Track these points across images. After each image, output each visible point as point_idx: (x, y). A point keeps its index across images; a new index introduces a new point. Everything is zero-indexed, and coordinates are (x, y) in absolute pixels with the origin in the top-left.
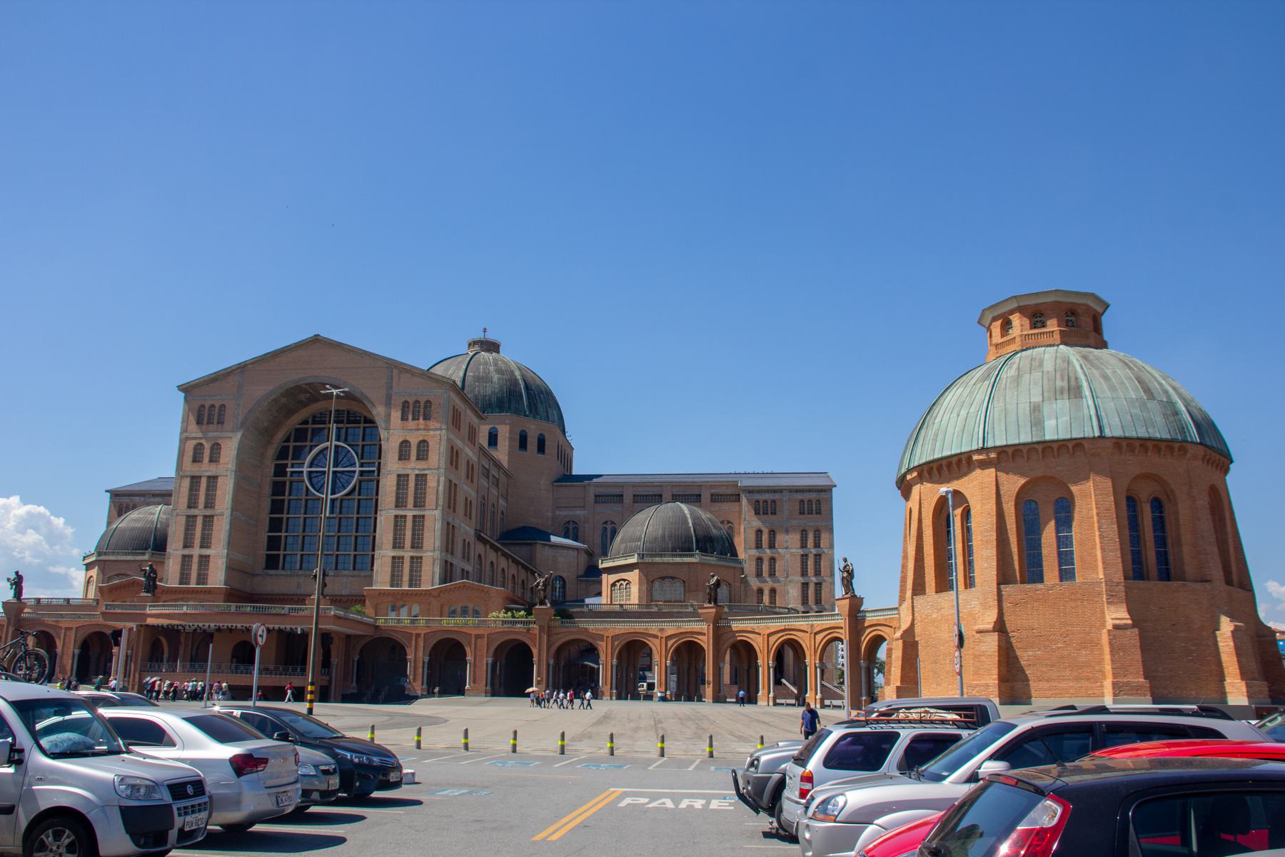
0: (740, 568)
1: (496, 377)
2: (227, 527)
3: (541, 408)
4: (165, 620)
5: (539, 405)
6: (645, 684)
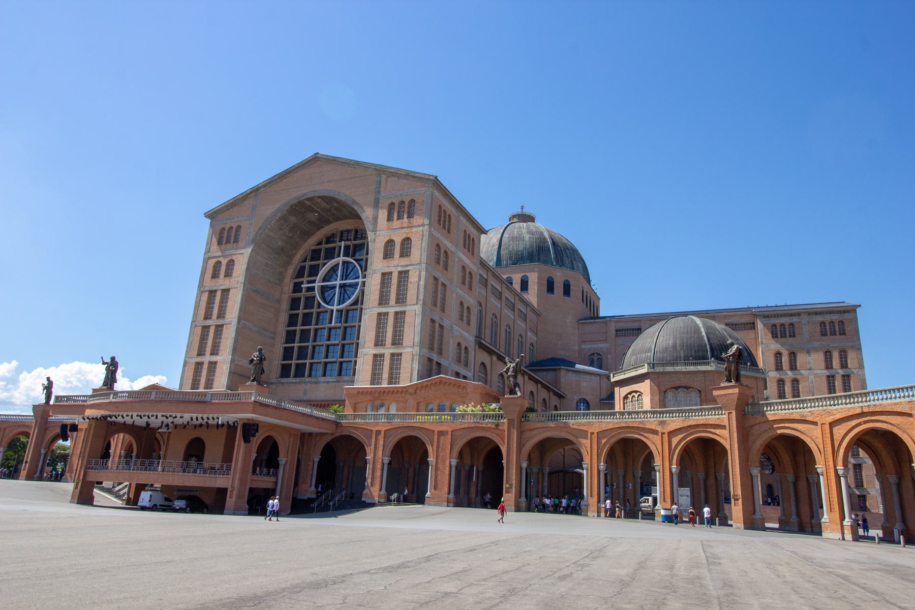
0: (762, 378)
1: (527, 237)
2: (233, 335)
3: (567, 261)
4: (100, 411)
5: (565, 258)
6: (650, 499)
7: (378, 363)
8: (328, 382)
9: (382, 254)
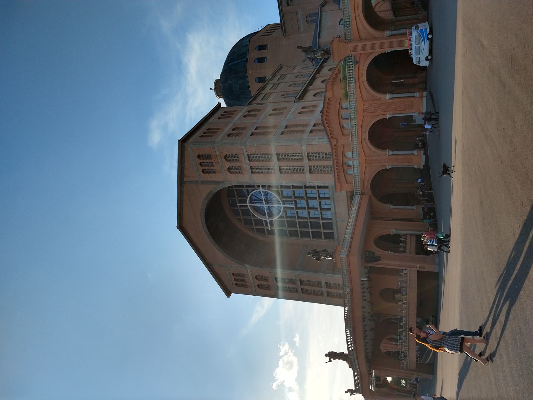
7: (316, 170)
8: (335, 206)
9: (238, 175)
